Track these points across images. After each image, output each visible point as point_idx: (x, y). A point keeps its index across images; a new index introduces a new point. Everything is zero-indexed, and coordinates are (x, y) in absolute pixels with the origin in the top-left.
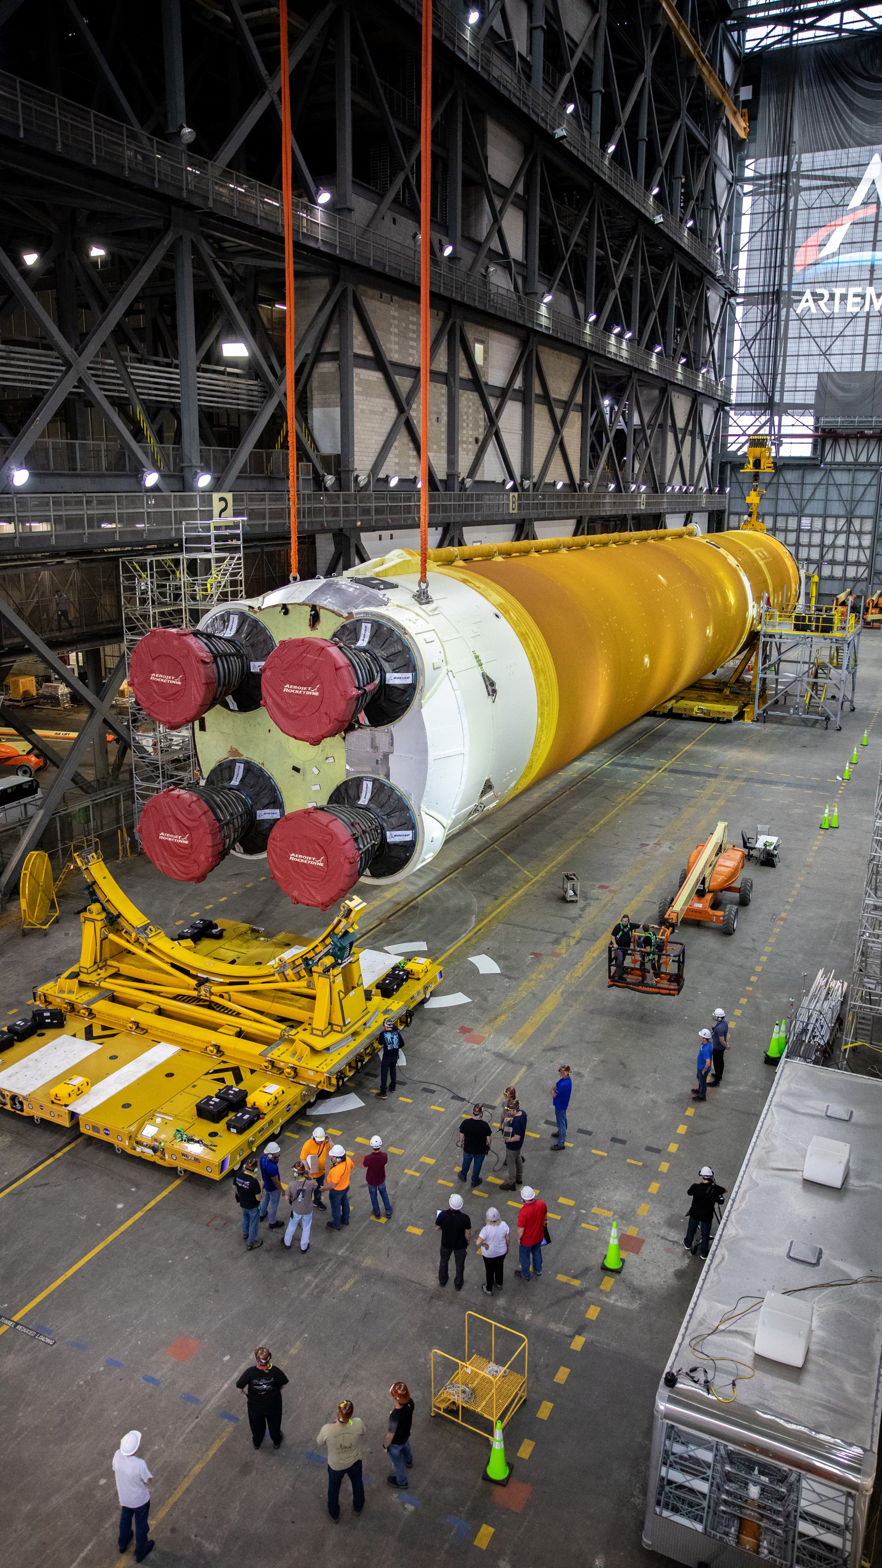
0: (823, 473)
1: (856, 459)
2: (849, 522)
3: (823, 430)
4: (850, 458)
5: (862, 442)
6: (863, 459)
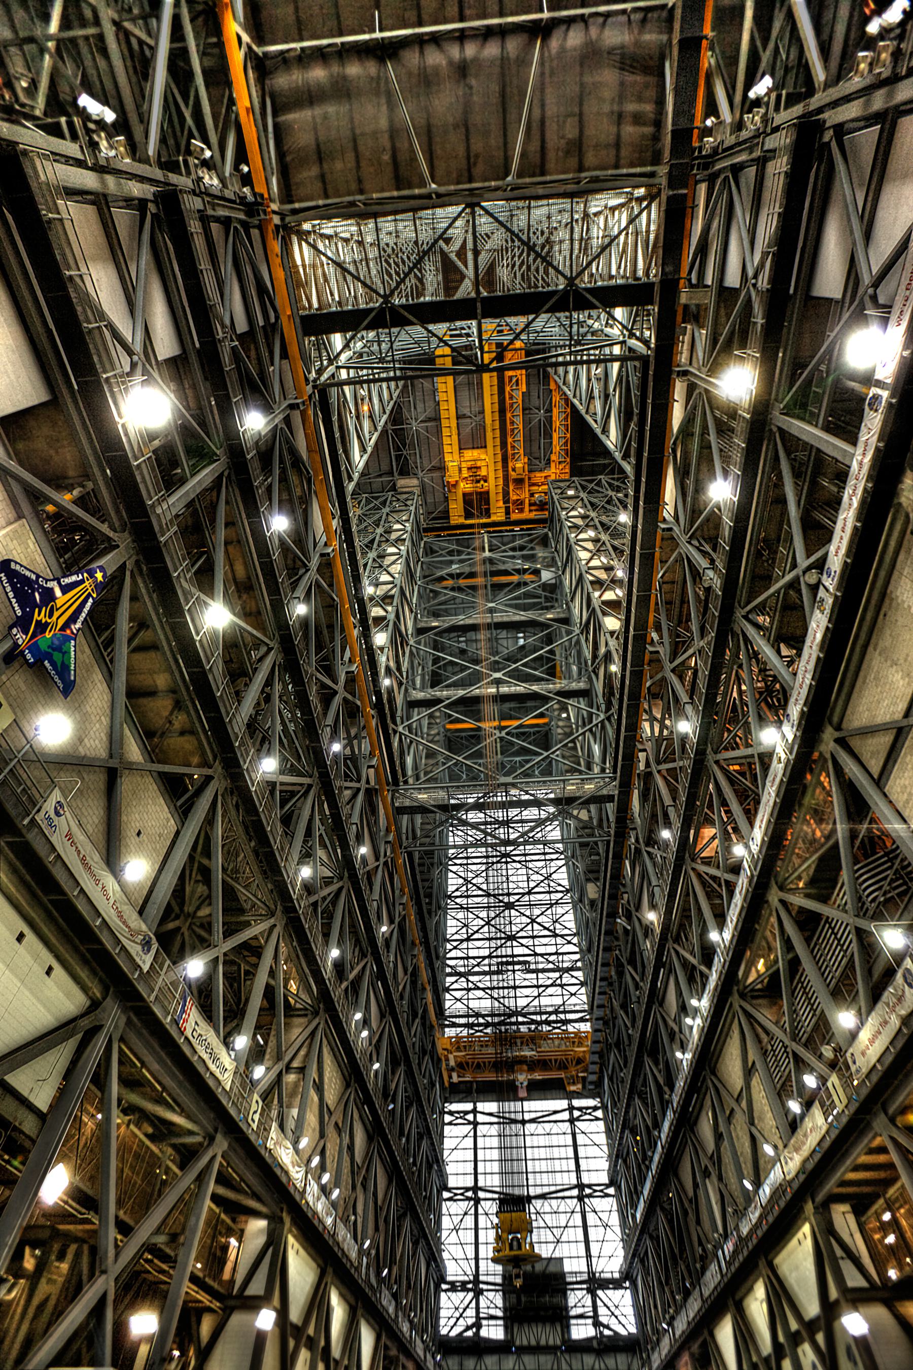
6: (543, 1342)
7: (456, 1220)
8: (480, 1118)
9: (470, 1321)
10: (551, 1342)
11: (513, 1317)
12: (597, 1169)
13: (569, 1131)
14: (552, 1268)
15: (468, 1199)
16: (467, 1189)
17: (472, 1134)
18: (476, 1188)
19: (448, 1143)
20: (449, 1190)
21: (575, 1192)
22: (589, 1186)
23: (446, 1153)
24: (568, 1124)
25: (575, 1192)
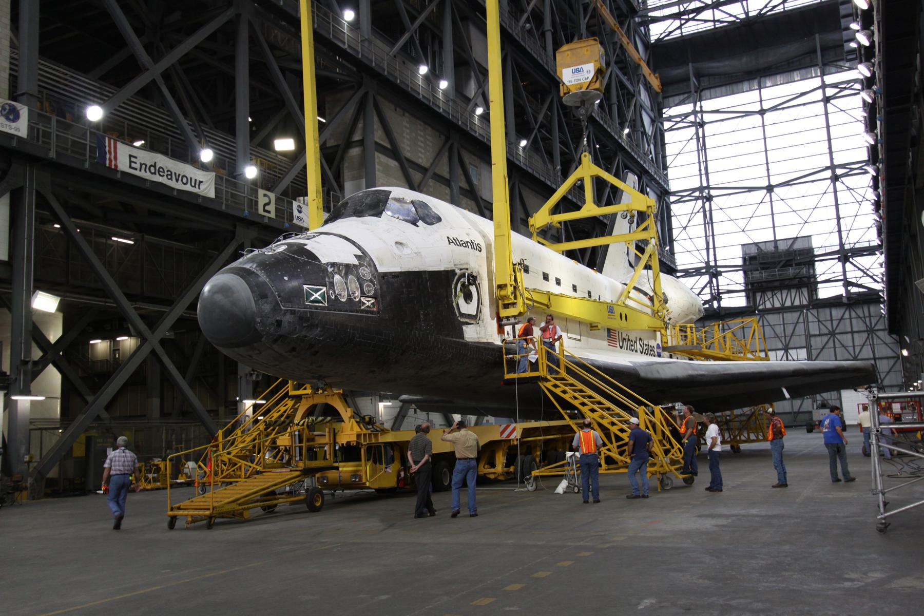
0: (758, 317)
1: (783, 304)
2: (786, 352)
3: (752, 284)
4: (777, 305)
5: (785, 292)
6: (788, 304)
8: (707, 118)
9: (708, 297)
10: (797, 303)
11: (752, 289)
14: (798, 246)
16: (694, 190)
20: (674, 194)
22: (843, 166)
25: (828, 173)
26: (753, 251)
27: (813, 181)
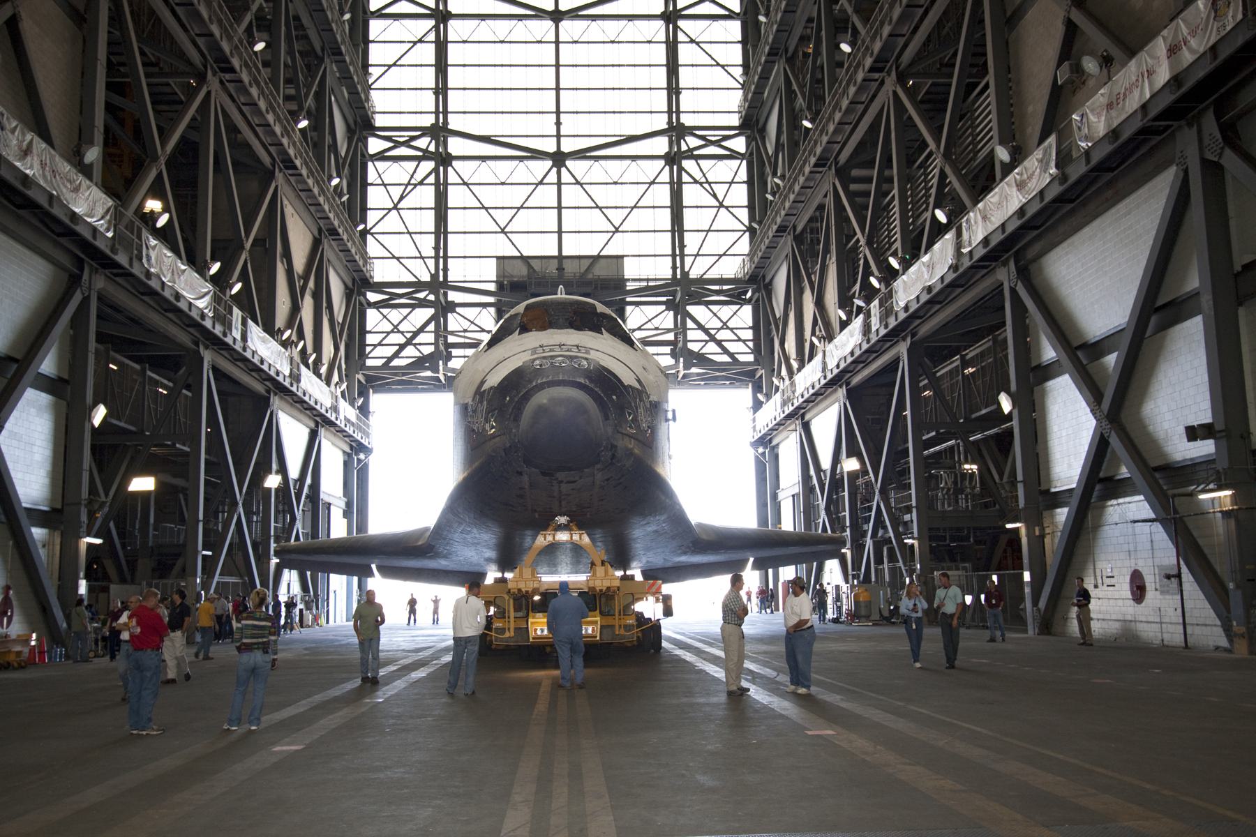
7: (396, 192)
9: (428, 350)
12: (716, 96)
13: (662, 36)
14: (600, 271)
15: (426, 155)
17: (432, 37)
18: (439, 131)
19: (377, 54)
21: (661, 145)
23: (375, 72)
24: (660, 24)
26: (521, 271)
27: (634, 158)
